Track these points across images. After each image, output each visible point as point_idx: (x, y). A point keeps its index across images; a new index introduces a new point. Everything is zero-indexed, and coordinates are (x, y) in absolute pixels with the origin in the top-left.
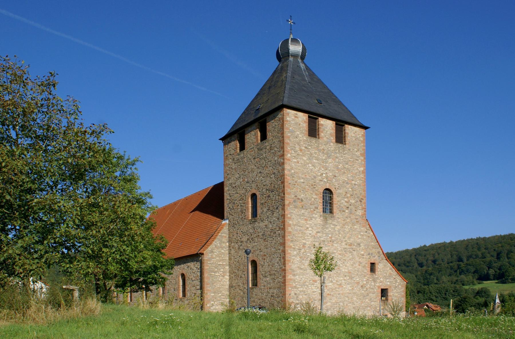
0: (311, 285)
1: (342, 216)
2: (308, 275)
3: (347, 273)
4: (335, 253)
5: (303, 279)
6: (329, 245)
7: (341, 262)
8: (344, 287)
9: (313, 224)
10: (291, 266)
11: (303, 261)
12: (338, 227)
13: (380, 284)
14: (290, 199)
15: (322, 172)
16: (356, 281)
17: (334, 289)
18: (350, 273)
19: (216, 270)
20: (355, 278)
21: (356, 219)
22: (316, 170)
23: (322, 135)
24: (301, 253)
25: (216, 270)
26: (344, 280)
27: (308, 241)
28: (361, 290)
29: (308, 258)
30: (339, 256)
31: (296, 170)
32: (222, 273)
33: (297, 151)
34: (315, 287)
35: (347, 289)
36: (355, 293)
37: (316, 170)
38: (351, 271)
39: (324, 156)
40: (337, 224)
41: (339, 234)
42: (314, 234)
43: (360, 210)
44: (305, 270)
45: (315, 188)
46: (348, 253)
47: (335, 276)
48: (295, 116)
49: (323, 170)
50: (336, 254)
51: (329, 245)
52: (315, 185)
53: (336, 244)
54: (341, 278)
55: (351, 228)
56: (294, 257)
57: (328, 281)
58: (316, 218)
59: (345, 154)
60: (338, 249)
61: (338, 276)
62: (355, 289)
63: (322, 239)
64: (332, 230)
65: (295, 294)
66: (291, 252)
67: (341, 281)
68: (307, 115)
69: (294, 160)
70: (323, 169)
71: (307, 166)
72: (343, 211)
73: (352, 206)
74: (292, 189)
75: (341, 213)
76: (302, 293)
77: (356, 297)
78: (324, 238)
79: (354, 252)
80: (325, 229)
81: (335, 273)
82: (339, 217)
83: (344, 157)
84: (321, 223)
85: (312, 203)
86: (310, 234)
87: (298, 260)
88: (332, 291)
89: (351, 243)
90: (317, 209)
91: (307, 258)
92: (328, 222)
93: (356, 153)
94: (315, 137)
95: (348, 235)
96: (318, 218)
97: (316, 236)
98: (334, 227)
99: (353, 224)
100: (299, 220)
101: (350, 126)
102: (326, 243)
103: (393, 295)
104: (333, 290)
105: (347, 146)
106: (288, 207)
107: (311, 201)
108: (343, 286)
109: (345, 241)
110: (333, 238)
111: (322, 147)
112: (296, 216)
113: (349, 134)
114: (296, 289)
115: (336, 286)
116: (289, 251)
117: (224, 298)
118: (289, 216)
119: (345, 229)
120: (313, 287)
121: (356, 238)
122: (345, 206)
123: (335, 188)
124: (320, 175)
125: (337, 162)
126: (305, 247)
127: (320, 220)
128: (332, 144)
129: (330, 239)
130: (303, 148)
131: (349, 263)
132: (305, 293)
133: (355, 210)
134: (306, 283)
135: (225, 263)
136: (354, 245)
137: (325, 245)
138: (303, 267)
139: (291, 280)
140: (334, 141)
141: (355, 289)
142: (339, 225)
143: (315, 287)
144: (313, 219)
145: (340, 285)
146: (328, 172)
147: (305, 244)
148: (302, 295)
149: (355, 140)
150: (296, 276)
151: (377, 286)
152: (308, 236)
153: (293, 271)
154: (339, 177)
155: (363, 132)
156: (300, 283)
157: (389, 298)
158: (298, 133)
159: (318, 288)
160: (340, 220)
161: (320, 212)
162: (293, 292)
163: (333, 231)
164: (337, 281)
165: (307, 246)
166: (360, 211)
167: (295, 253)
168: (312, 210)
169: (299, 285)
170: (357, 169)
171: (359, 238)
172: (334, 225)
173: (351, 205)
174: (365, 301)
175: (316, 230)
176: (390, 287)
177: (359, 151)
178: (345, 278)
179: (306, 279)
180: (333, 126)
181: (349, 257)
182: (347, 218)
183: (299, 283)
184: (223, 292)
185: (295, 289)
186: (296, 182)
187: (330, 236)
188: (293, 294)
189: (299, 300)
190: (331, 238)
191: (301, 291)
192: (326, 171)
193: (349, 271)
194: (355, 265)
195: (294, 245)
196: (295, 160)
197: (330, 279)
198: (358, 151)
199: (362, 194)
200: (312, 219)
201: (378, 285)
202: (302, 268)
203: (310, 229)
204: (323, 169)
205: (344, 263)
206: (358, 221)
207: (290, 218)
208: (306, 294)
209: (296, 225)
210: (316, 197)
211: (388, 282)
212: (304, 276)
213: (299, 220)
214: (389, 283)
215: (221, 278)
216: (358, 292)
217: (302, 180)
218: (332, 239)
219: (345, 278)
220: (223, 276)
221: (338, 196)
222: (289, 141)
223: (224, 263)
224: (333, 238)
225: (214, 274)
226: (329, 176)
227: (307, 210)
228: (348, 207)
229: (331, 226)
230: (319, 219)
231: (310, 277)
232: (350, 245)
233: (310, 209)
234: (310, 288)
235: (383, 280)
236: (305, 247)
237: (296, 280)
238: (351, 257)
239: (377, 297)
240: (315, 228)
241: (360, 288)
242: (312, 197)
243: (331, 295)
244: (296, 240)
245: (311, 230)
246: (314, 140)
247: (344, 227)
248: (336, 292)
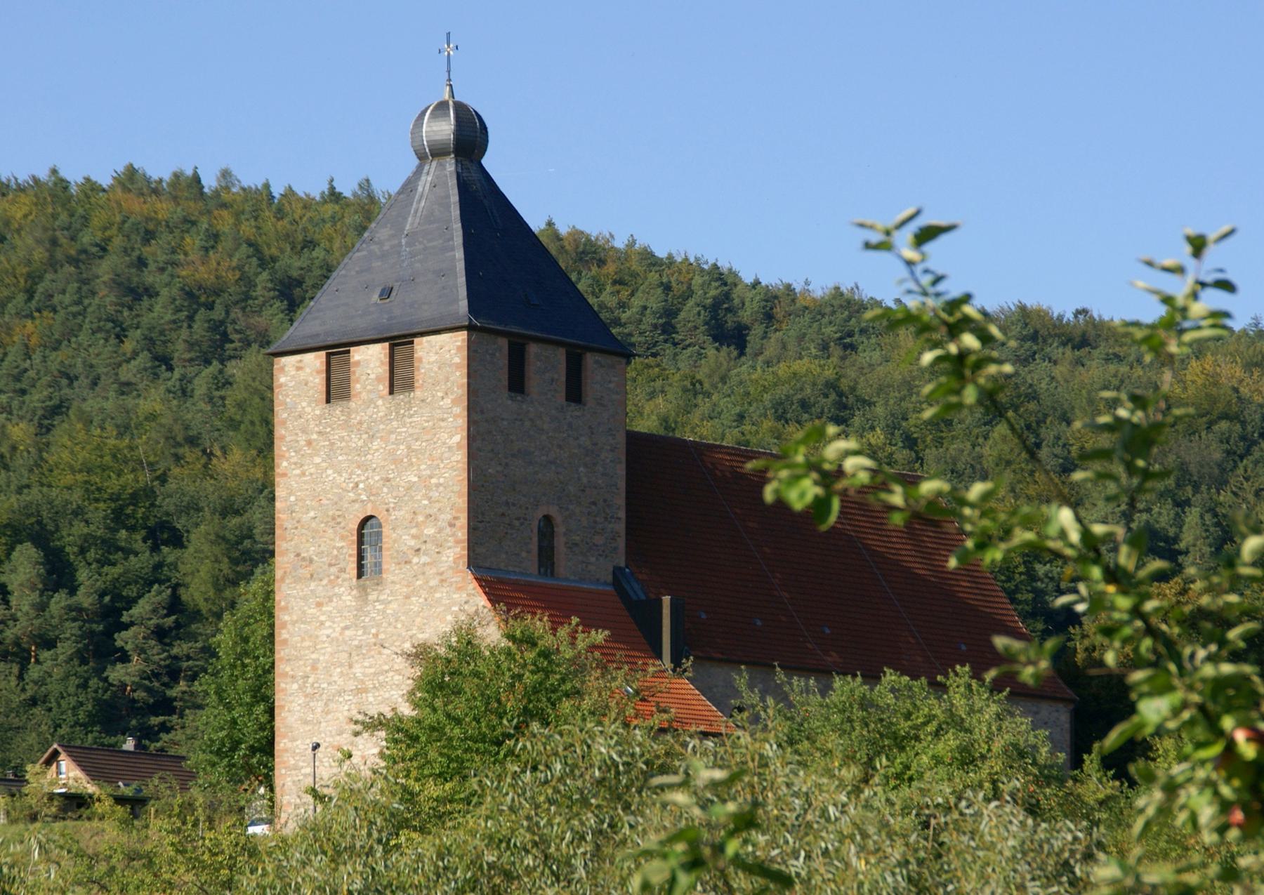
10: (285, 718)
11: (312, 704)
12: (394, 606)
23: (356, 387)
33: (300, 450)
39: (360, 439)
44: (315, 724)
45: (339, 523)
49: (358, 475)
55: (426, 600)
58: (340, 596)
63: (356, 643)
69: (294, 472)
70: (359, 472)
72: (406, 562)
73: (429, 546)
74: (291, 540)
78: (361, 640)
82: (395, 579)
86: (328, 636)
87: (300, 702)
91: (321, 695)
92: (370, 597)
95: (419, 620)
96: (346, 592)
97: (341, 638)
99: (433, 590)
102: (364, 652)
105: (418, 393)
110: (382, 636)
116: (283, 685)
122: (411, 548)
124: (353, 488)
125: (393, 443)
126: (317, 669)
127: (350, 598)
128: (380, 402)
129: (373, 640)
130: (315, 436)
138: (310, 717)
139: (286, 750)
147: (316, 661)
149: (439, 368)
152: (324, 642)
165: (320, 666)
167: (295, 686)
168: (332, 577)
169: (304, 761)
170: (444, 443)
185: (293, 772)
186: (298, 522)
187: (374, 631)
190: (376, 635)
195: (292, 670)
196: (297, 472)
200: (331, 601)
203: (328, 624)
204: (359, 472)
207: (286, 608)
209: (296, 622)
217: (312, 514)
222: (283, 432)
224: (382, 636)
228: (418, 550)
230: (349, 594)
234: (327, 764)
236: (317, 669)
237: (297, 751)
245: (330, 627)
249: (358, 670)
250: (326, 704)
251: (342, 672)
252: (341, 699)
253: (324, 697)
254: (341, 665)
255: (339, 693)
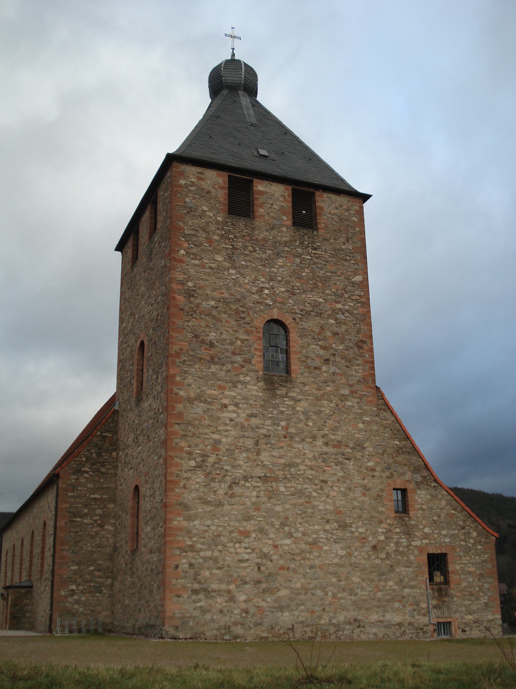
0: (235, 543)
1: (312, 379)
2: (226, 518)
3: (331, 513)
4: (297, 465)
5: (214, 528)
6: (282, 444)
7: (315, 487)
8: (325, 548)
9: (239, 397)
11: (213, 484)
13: (424, 541)
15: (262, 285)
16: (357, 534)
17: (298, 555)
18: (340, 512)
20: (354, 526)
21: (349, 385)
22: (247, 281)
24: (209, 465)
26: (325, 531)
27: (227, 436)
28: (373, 557)
29: (225, 476)
30: (309, 472)
31: (198, 282)
34: (246, 548)
35: (333, 555)
36: (354, 566)
37: (247, 281)
38: (342, 509)
40: (300, 397)
41: (307, 419)
42: (243, 420)
43: (358, 365)
45: (244, 318)
46: (332, 464)
47: (300, 520)
48: (198, 177)
49: (263, 282)
50: (302, 467)
51: (282, 444)
52: (243, 312)
53: (299, 442)
54: (316, 527)
55: (337, 406)
57: (281, 535)
58: (245, 383)
60: (304, 454)
61: (306, 522)
62: (356, 554)
63: (264, 431)
64: (288, 410)
65: (191, 565)
66: (183, 462)
67: (316, 533)
70: (263, 280)
71: (226, 273)
75: (310, 372)
76: (210, 563)
77: (359, 574)
78: (269, 430)
79: (347, 462)
80: (271, 409)
81: (298, 514)
82: (305, 380)
83: (315, 254)
84: (261, 394)
85: (237, 351)
86: (231, 420)
87: (199, 480)
88: (294, 559)
89: (338, 441)
90: (250, 363)
93: (344, 247)
95: (330, 422)
98: (292, 403)
99: (344, 399)
101: (325, 195)
102: (273, 442)
104: (296, 557)
107: (233, 347)
108: (321, 548)
109: (323, 437)
113: (325, 210)
114: (194, 553)
115: (303, 546)
118: (178, 378)
119: (322, 409)
120: (240, 547)
121: (350, 429)
123: (294, 319)
124: (257, 291)
126: (219, 450)
127: (256, 388)
128: (284, 229)
131: (335, 488)
132: (218, 563)
133: (347, 366)
134: (222, 538)
136: (347, 446)
137: (269, 446)
138: (211, 497)
139: (180, 529)
140: (290, 223)
141: (356, 554)
142: (307, 399)
143: (246, 548)
144: (239, 386)
145: (314, 543)
146: (275, 285)
147: (217, 442)
148: (209, 569)
150: (193, 521)
151: (416, 547)
152: (227, 425)
153: (187, 507)
154: (304, 296)
156: (204, 538)
158: (205, 208)
159: (253, 550)
160: (307, 388)
161: (256, 371)
162: (184, 561)
163: (291, 412)
164: (304, 534)
165: (223, 448)
166: (357, 368)
168: (236, 365)
169: (202, 544)
171: (361, 430)
172: (293, 399)
173: (334, 355)
174: (384, 587)
175: (247, 412)
176: (453, 549)
178: (327, 527)
179: (220, 529)
181: (336, 474)
183: (201, 538)
185: (190, 554)
187: (283, 423)
188: (186, 566)
189: (202, 581)
190: (286, 428)
191: (205, 559)
192: (271, 284)
193: (338, 507)
194: (351, 495)
195: (189, 446)
197: (287, 529)
199: (362, 331)
200: (235, 387)
201: (418, 543)
202: (210, 502)
203: (231, 408)
205: (321, 488)
206: (354, 389)
208: (220, 565)
210: (248, 337)
211: (445, 536)
212: (216, 521)
214: (447, 540)
216: (363, 562)
217: (213, 303)
218: (290, 431)
219: (327, 527)
221: (300, 336)
224: (292, 430)
226: (277, 292)
227: (224, 365)
228: (328, 360)
229: (286, 403)
230: (255, 385)
231: (231, 523)
232: (338, 444)
233: (232, 363)
234: (232, 550)
235: (430, 532)
236: (219, 450)
237: (195, 531)
238: (340, 474)
240: (245, 406)
241: (370, 553)
242: (237, 338)
243: (288, 569)
244: (194, 434)
246: (241, 223)
247: (319, 403)
248: (302, 562)
249: (265, 457)
250: (230, 487)
251: (248, 458)
252: (247, 484)
253: (228, 479)
254: (247, 450)
255: (246, 478)
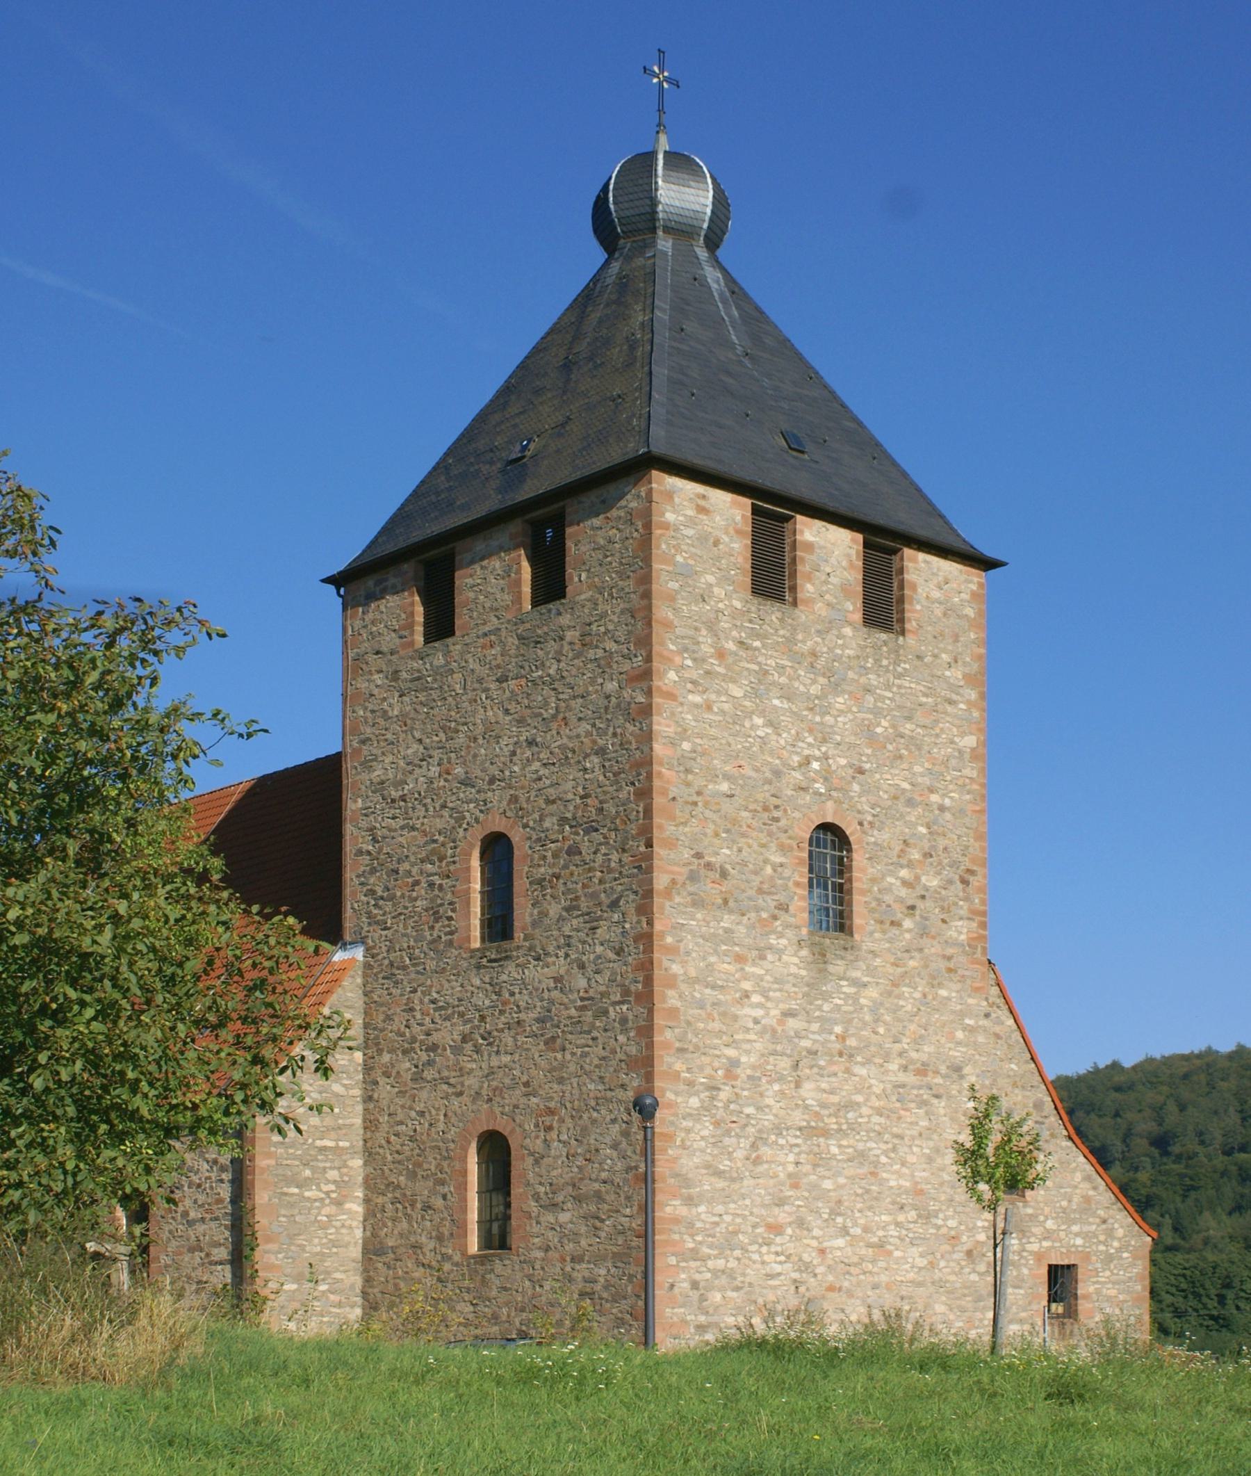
0: (761, 1246)
1: (887, 945)
2: (748, 1202)
3: (907, 1192)
4: (858, 1104)
5: (728, 1218)
6: (835, 1068)
7: (884, 1147)
8: (897, 1254)
9: (768, 978)
10: (675, 1160)
11: (727, 1141)
12: (872, 992)
13: (1046, 1244)
14: (676, 869)
15: (806, 752)
16: (944, 1230)
17: (855, 1265)
18: (921, 1192)
19: (308, 1173)
20: (941, 1215)
21: (944, 957)
22: (782, 742)
23: (807, 589)
24: (720, 1104)
25: (308, 1173)
26: (898, 1224)
27: (748, 1052)
28: (967, 1270)
29: (746, 1125)
30: (876, 1119)
31: (698, 741)
32: (332, 1187)
33: (704, 660)
34: (777, 1254)
35: (907, 1266)
36: (940, 1284)
37: (782, 742)
38: (924, 1186)
39: (814, 682)
40: (865, 979)
41: (876, 1021)
42: (774, 1022)
43: (961, 919)
44: (733, 1180)
45: (777, 820)
46: (913, 1105)
47: (859, 1206)
48: (698, 505)
49: (810, 745)
50: (865, 1110)
51: (835, 1068)
52: (776, 807)
53: (863, 1064)
54: (884, 1218)
55: (925, 996)
56: (686, 1124)
57: (832, 1230)
58: (780, 952)
59: (900, 676)
60: (870, 1087)
61: (870, 1208)
62: (942, 1264)
63: (805, 1043)
64: (846, 1004)
65: (695, 1285)
66: (679, 1100)
67: (884, 1228)
68: (747, 502)
69: (690, 697)
70: (810, 740)
71: (747, 724)
72: (892, 923)
73: (929, 904)
74: (685, 824)
75: (884, 932)
76: (724, 1280)
77: (944, 1298)
78: (815, 1041)
79: (935, 1101)
80: (819, 1002)
81: (857, 1195)
83: (900, 687)
84: (803, 973)
85: (765, 886)
86: (756, 1021)
87: (705, 1133)
88: (848, 1273)
89: (923, 1064)
90: (787, 910)
92: (831, 968)
93: (948, 673)
94: (781, 599)
95: (913, 1027)
97: (779, 1029)
98: (852, 990)
99: (935, 982)
100: (713, 959)
101: (922, 556)
102: (822, 1063)
103: (1098, 1292)
104: (852, 1269)
105: (911, 640)
106: (668, 904)
107: (758, 879)
108: (890, 1253)
109: (900, 1055)
110: (852, 1042)
111: (809, 643)
112: (701, 941)
113: (920, 590)
114: (698, 1263)
115: (863, 1252)
116: (670, 1096)
117: (340, 1305)
118: (669, 940)
119: (902, 1003)
120: (769, 1253)
121: (943, 1040)
122: (900, 900)
123: (861, 824)
124: (800, 765)
125: (870, 711)
126: (736, 1078)
127: (796, 960)
128: (848, 631)
129: (838, 1046)
130: (731, 646)
131: (915, 1149)
132: (735, 1279)
133: (944, 921)
134: (740, 1236)
135: (347, 1144)
136: (937, 1072)
137: (815, 1070)
138: (724, 1165)
139: (676, 1220)
140: (858, 617)
141: (942, 1264)
142: (877, 983)
143: (777, 1254)
144: (770, 957)
145: (881, 1245)
146: (830, 753)
147: (735, 1063)
148: (722, 1289)
149: (945, 614)
150: (696, 1206)
151: (1031, 1252)
152: (747, 1030)
153: (686, 1182)
154: (877, 776)
155: (976, 580)
156: (714, 1236)
157: (1080, 1308)
158: (710, 579)
159: (788, 1257)
160: (878, 962)
161: (797, 927)
162: (683, 1276)
163: (851, 1008)
164: (866, 1229)
165: (744, 1073)
166: (960, 923)
167: (694, 1102)
168: (764, 915)
169: (711, 1246)
170: (952, 742)
171: (959, 1043)
172: (855, 982)
173: (923, 897)
174: (981, 1320)
175: (781, 1006)
176: (1087, 1257)
177: (960, 663)
178: (901, 1218)
179: (738, 1220)
180: (853, 552)
181: (917, 1123)
182: (906, 955)
183: (709, 1236)
184: (338, 1275)
185: (693, 1264)
186: (699, 793)
187: (838, 1029)
188: (686, 1285)
189: (711, 1310)
190: (842, 1038)
191: (716, 1273)
192: (824, 749)
193: (917, 1183)
194: (939, 1161)
195: (689, 1070)
196: (696, 699)
197: (839, 1220)
198: (956, 661)
199: (971, 849)
200: (763, 958)
201: (1034, 1247)
202: (724, 1172)
203: (756, 998)
204: (810, 740)
205: (894, 1149)
206: (952, 966)
207: (672, 951)
208: (737, 1283)
209: (696, 980)
210: (783, 860)
211: (1077, 1235)
212: (732, 1206)
213: (713, 959)
214: (1079, 1241)
215: (326, 1210)
216: (952, 1278)
217: (724, 787)
218: (848, 1043)
219: (901, 1218)
220: (339, 1203)
221: (870, 859)
222: (670, 615)
223: (341, 1144)
224: (852, 1042)
225: (296, 1190)
226: (834, 768)
227: (743, 915)
228: (912, 908)
229: (845, 989)
230: (795, 955)
231: (755, 1210)
232: (922, 1071)
233: (758, 910)
234: (756, 1257)
235: (1055, 1227)
236: (736, 1078)
237: (699, 1225)
238: (924, 1123)
239: (1030, 1303)
240: (778, 994)
241: (963, 1263)
242: (766, 861)
243: (840, 1289)
244: (697, 1048)
246: (773, 612)
247: (897, 991)
248: (862, 1277)
249: (808, 1091)
250: (754, 1146)
251: (782, 1092)
252: (782, 1141)
253: (751, 1130)
254: (781, 1079)
255: (778, 1130)
